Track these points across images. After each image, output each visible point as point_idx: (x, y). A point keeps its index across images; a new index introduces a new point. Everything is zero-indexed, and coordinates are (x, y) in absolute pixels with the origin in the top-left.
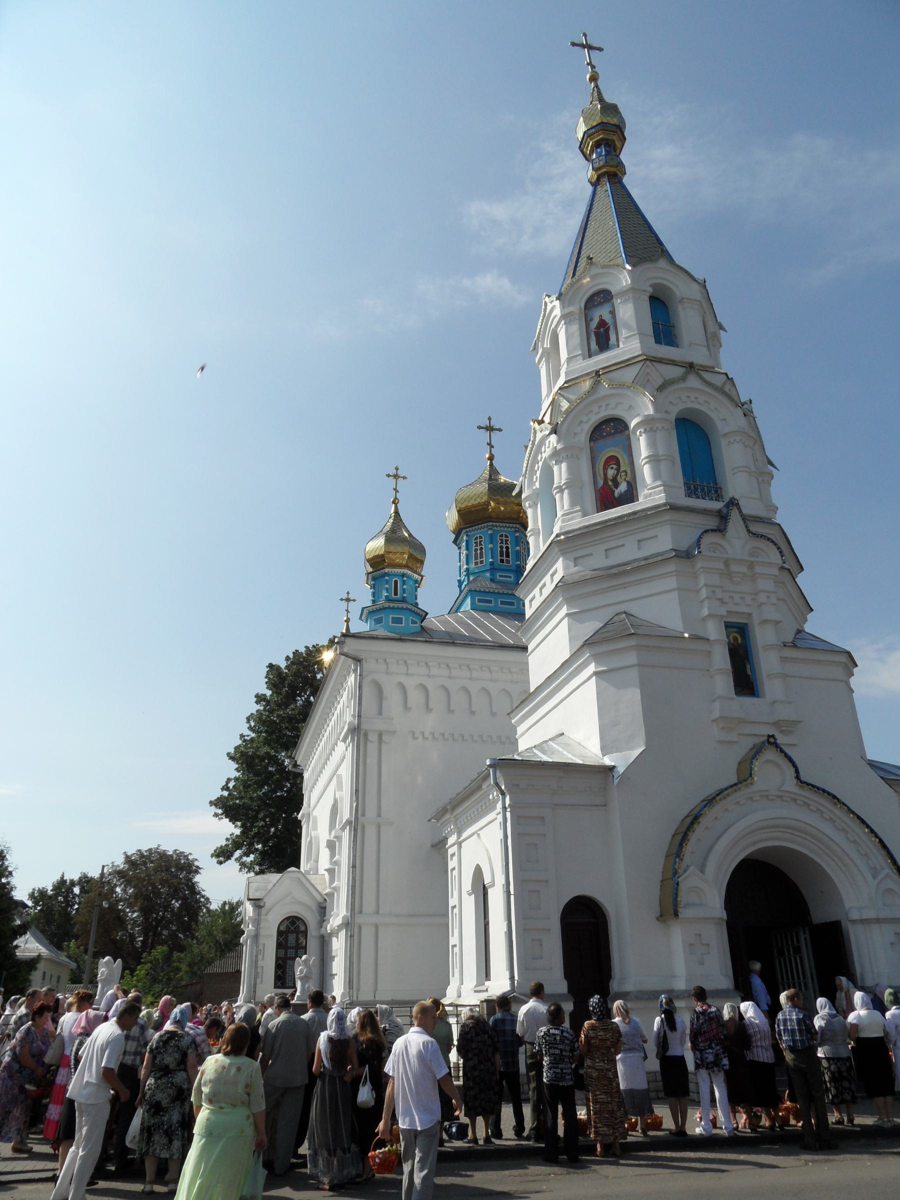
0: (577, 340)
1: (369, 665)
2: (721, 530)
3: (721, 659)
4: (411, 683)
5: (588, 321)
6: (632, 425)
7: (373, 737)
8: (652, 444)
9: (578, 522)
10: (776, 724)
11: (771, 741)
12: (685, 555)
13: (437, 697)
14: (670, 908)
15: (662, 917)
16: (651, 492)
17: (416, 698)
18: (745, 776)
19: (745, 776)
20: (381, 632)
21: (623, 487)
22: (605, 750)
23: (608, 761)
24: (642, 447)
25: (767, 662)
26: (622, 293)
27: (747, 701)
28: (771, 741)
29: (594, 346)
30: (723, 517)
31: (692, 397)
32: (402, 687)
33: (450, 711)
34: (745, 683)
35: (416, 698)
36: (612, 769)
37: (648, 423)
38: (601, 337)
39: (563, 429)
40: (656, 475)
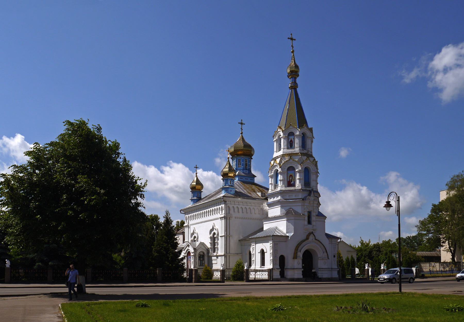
0: (286, 144)
1: (227, 202)
2: (309, 195)
3: (306, 218)
4: (235, 206)
5: (288, 139)
6: (297, 170)
7: (228, 218)
8: (300, 176)
9: (284, 188)
10: (313, 230)
11: (312, 233)
12: (303, 199)
13: (240, 210)
14: (295, 257)
15: (294, 258)
16: (298, 185)
17: (236, 210)
18: (307, 238)
19: (307, 238)
20: (230, 195)
21: (293, 182)
22: (287, 233)
23: (287, 235)
24: (298, 177)
25: (313, 218)
26: (297, 136)
27: (309, 225)
28: (312, 233)
29: (289, 146)
30: (310, 192)
31: (308, 164)
32: (233, 207)
33: (243, 213)
34: (309, 222)
35: (236, 210)
36: (288, 236)
37: (299, 172)
38: (291, 145)
39: (282, 167)
40: (300, 182)
